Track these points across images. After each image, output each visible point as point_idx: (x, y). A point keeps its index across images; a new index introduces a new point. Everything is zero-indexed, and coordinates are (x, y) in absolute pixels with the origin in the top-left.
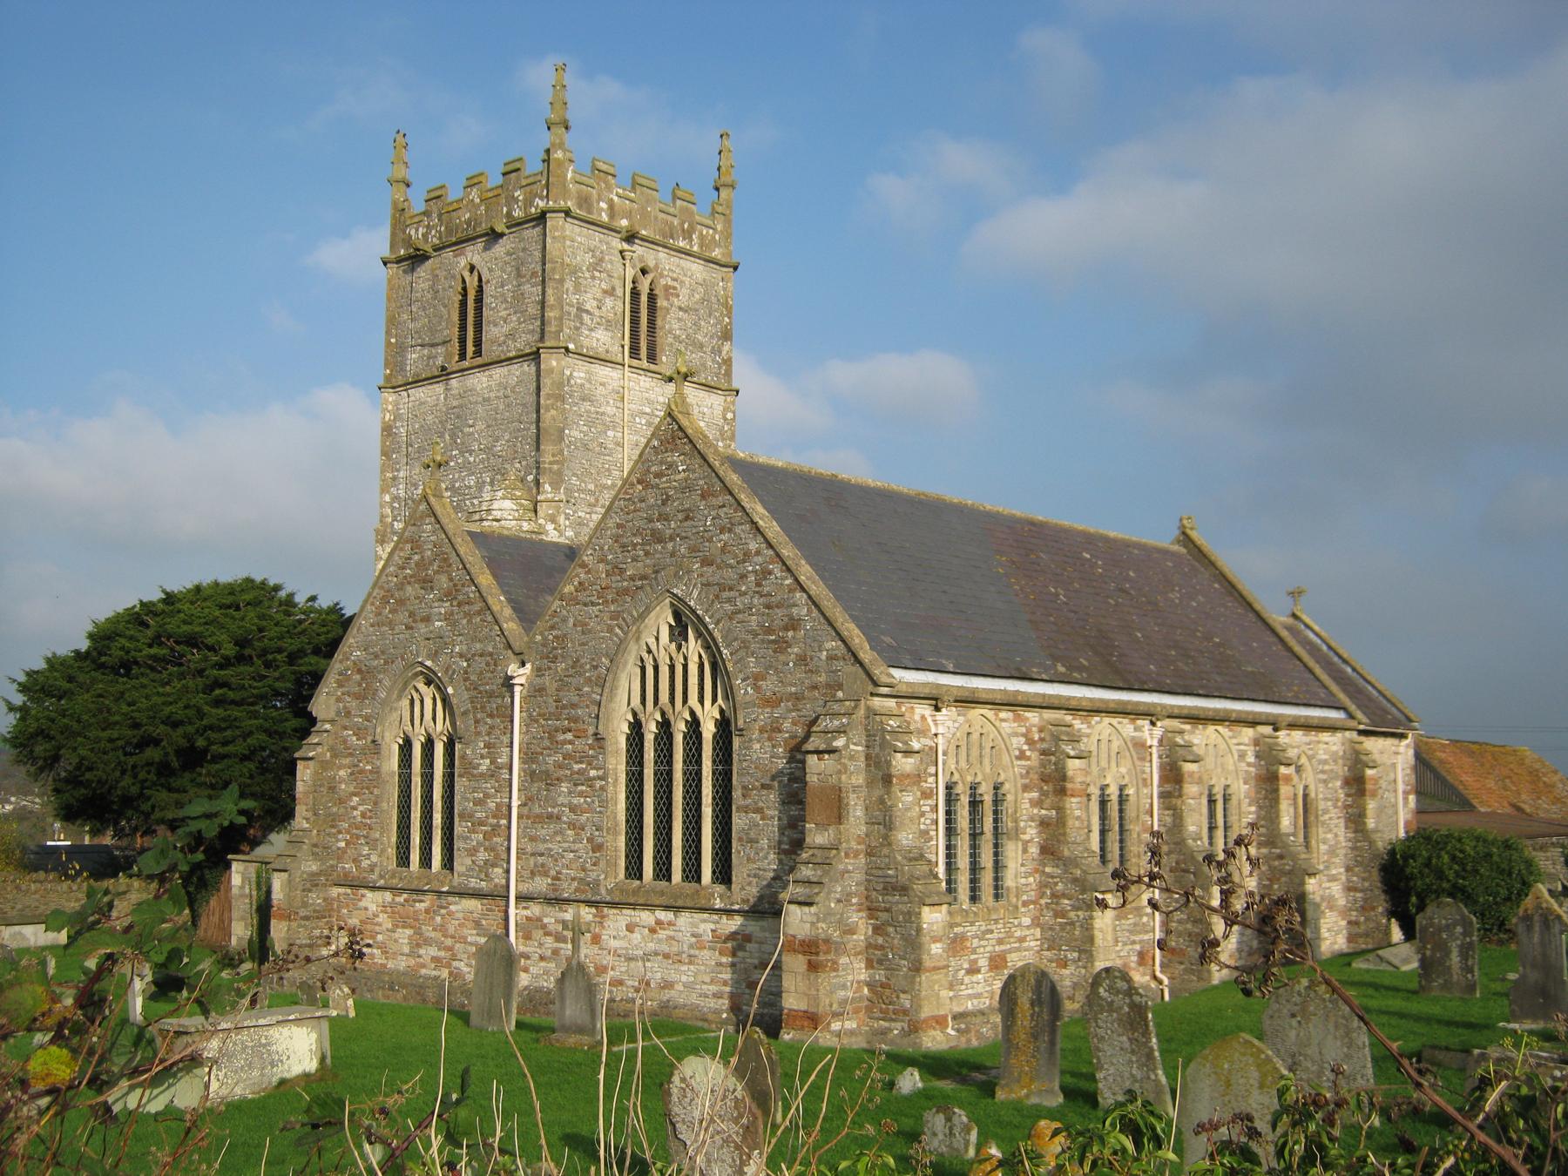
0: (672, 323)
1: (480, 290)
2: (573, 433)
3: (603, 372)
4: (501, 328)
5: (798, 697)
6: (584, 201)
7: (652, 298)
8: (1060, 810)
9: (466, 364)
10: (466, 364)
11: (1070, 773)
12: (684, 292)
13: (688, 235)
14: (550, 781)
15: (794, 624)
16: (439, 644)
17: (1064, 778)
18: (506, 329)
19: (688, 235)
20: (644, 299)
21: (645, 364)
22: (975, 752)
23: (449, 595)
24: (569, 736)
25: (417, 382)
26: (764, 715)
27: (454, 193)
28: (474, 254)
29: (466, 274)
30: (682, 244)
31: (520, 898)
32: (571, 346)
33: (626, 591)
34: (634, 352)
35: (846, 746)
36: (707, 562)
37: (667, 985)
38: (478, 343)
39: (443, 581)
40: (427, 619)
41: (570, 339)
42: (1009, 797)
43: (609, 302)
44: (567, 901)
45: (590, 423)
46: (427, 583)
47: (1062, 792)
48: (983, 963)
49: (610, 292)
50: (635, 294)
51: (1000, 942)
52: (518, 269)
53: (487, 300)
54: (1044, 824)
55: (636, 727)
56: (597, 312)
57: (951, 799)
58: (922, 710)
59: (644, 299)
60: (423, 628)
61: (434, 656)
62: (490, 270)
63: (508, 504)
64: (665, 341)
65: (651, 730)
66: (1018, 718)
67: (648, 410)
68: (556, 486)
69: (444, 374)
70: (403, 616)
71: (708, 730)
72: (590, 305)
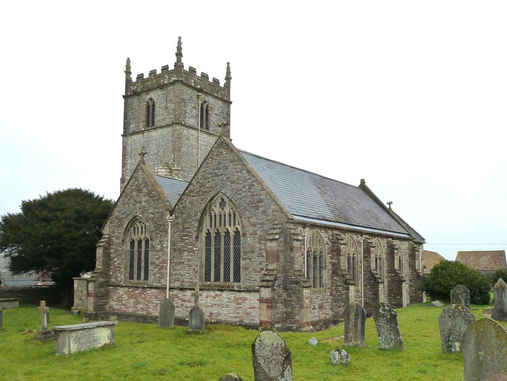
1: (154, 105)
2: (183, 149)
3: (193, 132)
4: (160, 116)
5: (262, 224)
6: (187, 79)
7: (207, 110)
8: (339, 260)
9: (150, 128)
10: (150, 128)
11: (341, 249)
12: (216, 110)
13: (217, 92)
14: (181, 251)
15: (261, 201)
16: (144, 210)
17: (340, 250)
18: (163, 117)
19: (217, 92)
20: (205, 110)
21: (205, 130)
22: (315, 241)
23: (149, 194)
24: (187, 238)
25: (134, 133)
26: (251, 230)
27: (146, 76)
28: (153, 95)
29: (149, 101)
31: (171, 289)
32: (183, 123)
33: (206, 192)
34: (202, 126)
35: (279, 238)
36: (233, 182)
37: (219, 314)
38: (153, 122)
39: (145, 190)
40: (140, 202)
41: (183, 121)
42: (324, 256)
43: (194, 110)
44: (186, 289)
46: (140, 191)
47: (339, 255)
48: (317, 306)
49: (194, 108)
50: (202, 109)
51: (322, 300)
52: (166, 99)
53: (156, 108)
54: (333, 264)
55: (209, 234)
56: (190, 113)
57: (308, 256)
58: (300, 228)
59: (205, 110)
60: (138, 205)
61: (142, 213)
62: (157, 99)
63: (163, 170)
65: (213, 235)
66: (326, 232)
68: (178, 166)
69: (143, 132)
70: (132, 202)
71: (232, 234)
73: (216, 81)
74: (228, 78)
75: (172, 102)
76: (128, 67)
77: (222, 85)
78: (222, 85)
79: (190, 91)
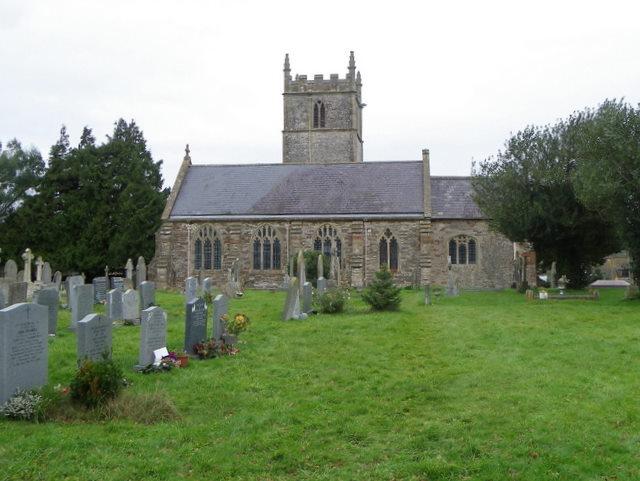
0: (330, 114)
7: (323, 108)
13: (335, 87)
19: (335, 87)
34: (316, 125)
50: (316, 109)
64: (327, 120)
72: (298, 116)
73: (334, 77)
74: (352, 67)
75: (323, 106)
77: (342, 76)
78: (342, 76)
79: (300, 98)
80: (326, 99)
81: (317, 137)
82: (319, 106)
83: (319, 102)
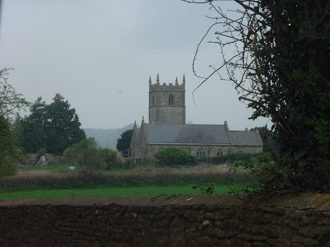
0: (175, 100)
30: (176, 90)
34: (170, 104)
41: (160, 104)
43: (165, 99)
45: (163, 113)
50: (170, 97)
67: (171, 111)
72: (163, 100)
76: (150, 81)
80: (174, 93)
81: (170, 109)
82: (171, 96)
83: (171, 94)
